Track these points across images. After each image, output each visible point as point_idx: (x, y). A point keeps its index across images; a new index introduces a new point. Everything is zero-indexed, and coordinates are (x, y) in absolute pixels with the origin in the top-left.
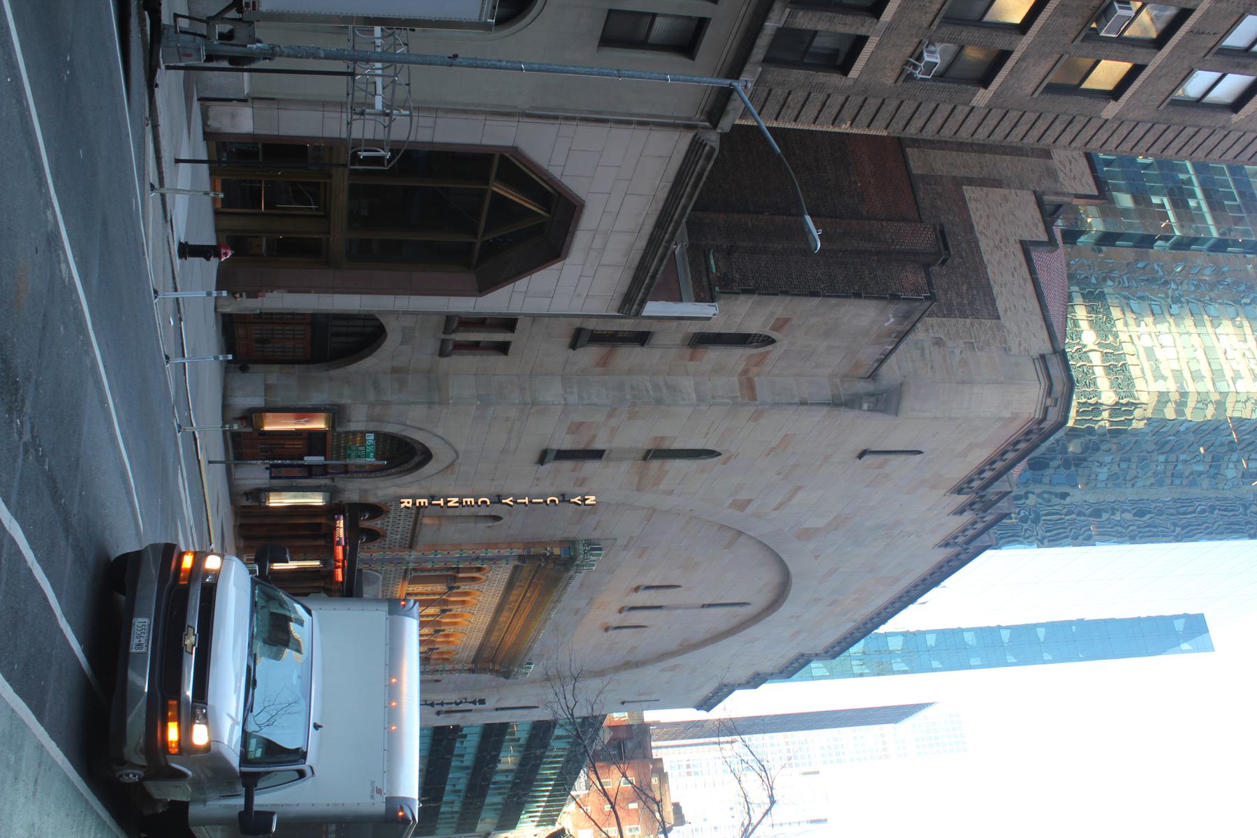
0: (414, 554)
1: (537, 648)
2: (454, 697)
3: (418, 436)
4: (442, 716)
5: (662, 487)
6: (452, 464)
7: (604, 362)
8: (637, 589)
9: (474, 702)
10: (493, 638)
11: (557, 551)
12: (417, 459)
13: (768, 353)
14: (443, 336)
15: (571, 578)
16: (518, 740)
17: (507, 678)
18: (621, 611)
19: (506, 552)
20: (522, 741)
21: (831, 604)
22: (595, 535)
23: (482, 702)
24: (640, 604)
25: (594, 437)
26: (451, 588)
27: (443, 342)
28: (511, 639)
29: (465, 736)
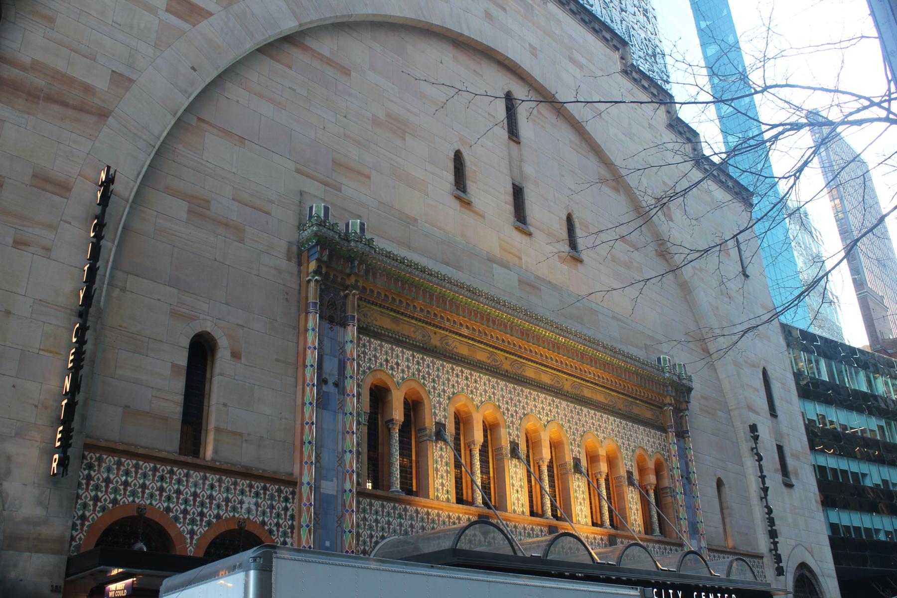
0: (307, 476)
1: (641, 355)
2: (750, 463)
4: (794, 481)
5: (100, 82)
8: (466, 204)
9: (756, 438)
10: (600, 398)
11: (313, 266)
15: (388, 255)
16: (881, 428)
17: (690, 389)
18: (529, 234)
19: (312, 338)
20: (883, 423)
21: (504, 10)
22: (286, 216)
23: (753, 428)
24: (510, 208)
26: (440, 435)
28: (592, 372)
29: (885, 482)
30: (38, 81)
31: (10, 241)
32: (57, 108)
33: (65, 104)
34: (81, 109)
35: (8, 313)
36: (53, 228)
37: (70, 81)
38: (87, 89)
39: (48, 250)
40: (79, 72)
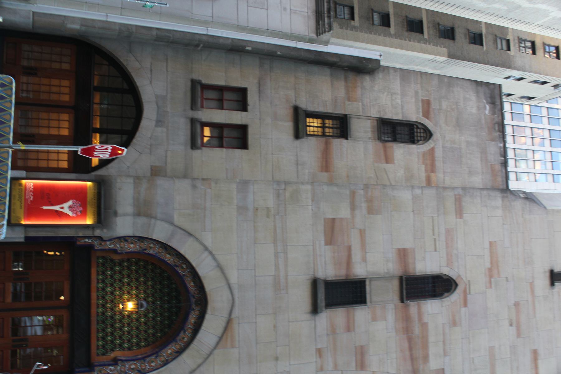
3: (188, 249)
6: (229, 321)
7: (326, 164)
12: (192, 319)
13: (433, 149)
14: (191, 114)
25: (349, 249)
27: (193, 121)
30: (417, 330)
31: (319, 347)
32: (406, 345)
33: (411, 349)
34: (412, 359)
35: (277, 359)
36: (336, 367)
37: (425, 346)
38: (426, 358)
39: (322, 369)
40: (432, 350)
